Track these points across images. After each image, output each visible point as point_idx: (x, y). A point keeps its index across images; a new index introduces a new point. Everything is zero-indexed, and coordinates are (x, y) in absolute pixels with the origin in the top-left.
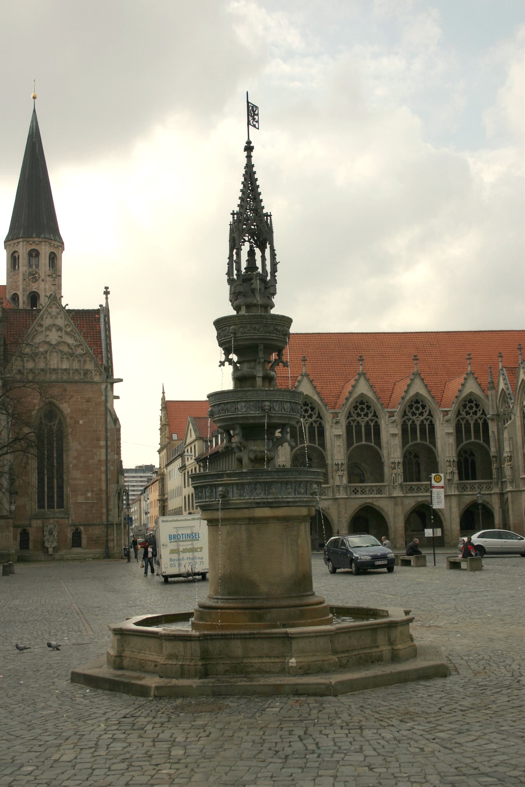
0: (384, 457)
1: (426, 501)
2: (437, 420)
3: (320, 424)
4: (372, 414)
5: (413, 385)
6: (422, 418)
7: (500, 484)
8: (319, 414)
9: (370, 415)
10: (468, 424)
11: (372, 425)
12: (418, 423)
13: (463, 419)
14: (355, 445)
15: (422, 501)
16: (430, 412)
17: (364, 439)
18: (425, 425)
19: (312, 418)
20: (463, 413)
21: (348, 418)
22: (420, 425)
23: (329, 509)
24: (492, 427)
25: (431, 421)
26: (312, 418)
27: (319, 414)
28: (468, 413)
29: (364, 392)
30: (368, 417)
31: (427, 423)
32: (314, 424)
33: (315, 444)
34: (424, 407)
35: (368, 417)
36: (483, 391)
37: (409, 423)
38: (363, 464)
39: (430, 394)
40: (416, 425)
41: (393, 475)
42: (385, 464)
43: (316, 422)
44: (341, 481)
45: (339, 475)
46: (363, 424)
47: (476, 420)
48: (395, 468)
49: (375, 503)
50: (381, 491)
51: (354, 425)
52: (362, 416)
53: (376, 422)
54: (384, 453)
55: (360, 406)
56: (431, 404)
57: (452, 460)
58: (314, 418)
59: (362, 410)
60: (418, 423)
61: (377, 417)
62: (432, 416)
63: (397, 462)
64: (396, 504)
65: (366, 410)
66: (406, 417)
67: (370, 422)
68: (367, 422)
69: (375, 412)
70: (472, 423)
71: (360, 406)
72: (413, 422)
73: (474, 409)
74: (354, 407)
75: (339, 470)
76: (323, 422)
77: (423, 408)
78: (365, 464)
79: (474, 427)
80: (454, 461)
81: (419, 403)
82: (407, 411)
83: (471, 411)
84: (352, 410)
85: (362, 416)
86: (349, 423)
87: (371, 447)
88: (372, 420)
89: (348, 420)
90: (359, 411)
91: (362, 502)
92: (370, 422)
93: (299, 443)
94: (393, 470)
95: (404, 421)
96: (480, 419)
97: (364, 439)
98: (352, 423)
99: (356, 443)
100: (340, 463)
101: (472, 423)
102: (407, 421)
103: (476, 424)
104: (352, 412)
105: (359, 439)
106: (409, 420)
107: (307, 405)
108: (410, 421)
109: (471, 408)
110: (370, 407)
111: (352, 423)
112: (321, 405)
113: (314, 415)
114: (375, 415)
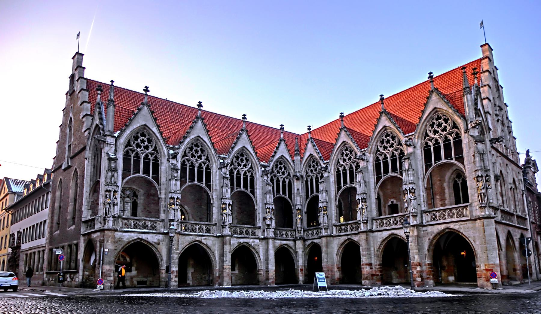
0: (213, 199)
1: (246, 243)
2: (257, 173)
3: (156, 157)
4: (205, 158)
5: (241, 139)
6: (246, 169)
7: (302, 232)
8: (156, 147)
9: (203, 158)
10: (278, 180)
11: (204, 167)
12: (242, 173)
13: (275, 176)
14: (188, 183)
15: (244, 243)
16: (251, 165)
17: (196, 179)
18: (247, 176)
19: (148, 150)
20: (276, 171)
21: (183, 157)
22: (244, 175)
23: (159, 244)
24: (298, 186)
25: (252, 174)
26: (148, 150)
27: (156, 147)
28: (278, 172)
29: (200, 135)
30: (201, 159)
31: (249, 175)
32: (150, 157)
33: (149, 176)
34: (247, 160)
35: (201, 159)
36: (291, 156)
37: (236, 172)
38: (186, 207)
39: (254, 150)
40: (240, 174)
41: (225, 216)
42: (214, 205)
43: (152, 154)
44: (176, 216)
45: (174, 209)
46: (197, 165)
47: (284, 179)
48: (226, 209)
49: (203, 241)
50: (210, 230)
51: (188, 164)
52: (196, 157)
53: (208, 166)
54: (215, 195)
55: (195, 148)
56: (254, 158)
57: (271, 208)
58: (150, 150)
59: (197, 152)
60: (242, 173)
61: (209, 161)
62: (253, 169)
63: (228, 203)
64: (223, 244)
65: (200, 153)
66: (233, 166)
67: (203, 164)
68: (200, 164)
69: (207, 157)
70: (281, 180)
71: (195, 148)
72: (238, 171)
73: (283, 170)
74: (189, 148)
75: (174, 204)
76: (158, 156)
77: (247, 161)
78: (198, 201)
79: (283, 184)
80: (272, 209)
81: (243, 156)
82: (234, 161)
83: (281, 171)
84: (188, 150)
85: (196, 157)
86: (184, 162)
87: (201, 187)
88: (205, 163)
89: (183, 159)
90: (193, 152)
91: (193, 238)
92: (203, 164)
93: (132, 173)
94: (223, 210)
95: (231, 170)
96: (287, 178)
97: (196, 179)
98: (186, 162)
99: (189, 182)
100: (176, 197)
101: (281, 180)
102: (234, 170)
103: (284, 181)
104: (187, 152)
105: (192, 179)
106: (235, 169)
107: (145, 136)
108: (236, 170)
109: (281, 168)
110: (204, 151)
111: (186, 162)
112: (160, 139)
113: (150, 147)
114: (207, 159)
